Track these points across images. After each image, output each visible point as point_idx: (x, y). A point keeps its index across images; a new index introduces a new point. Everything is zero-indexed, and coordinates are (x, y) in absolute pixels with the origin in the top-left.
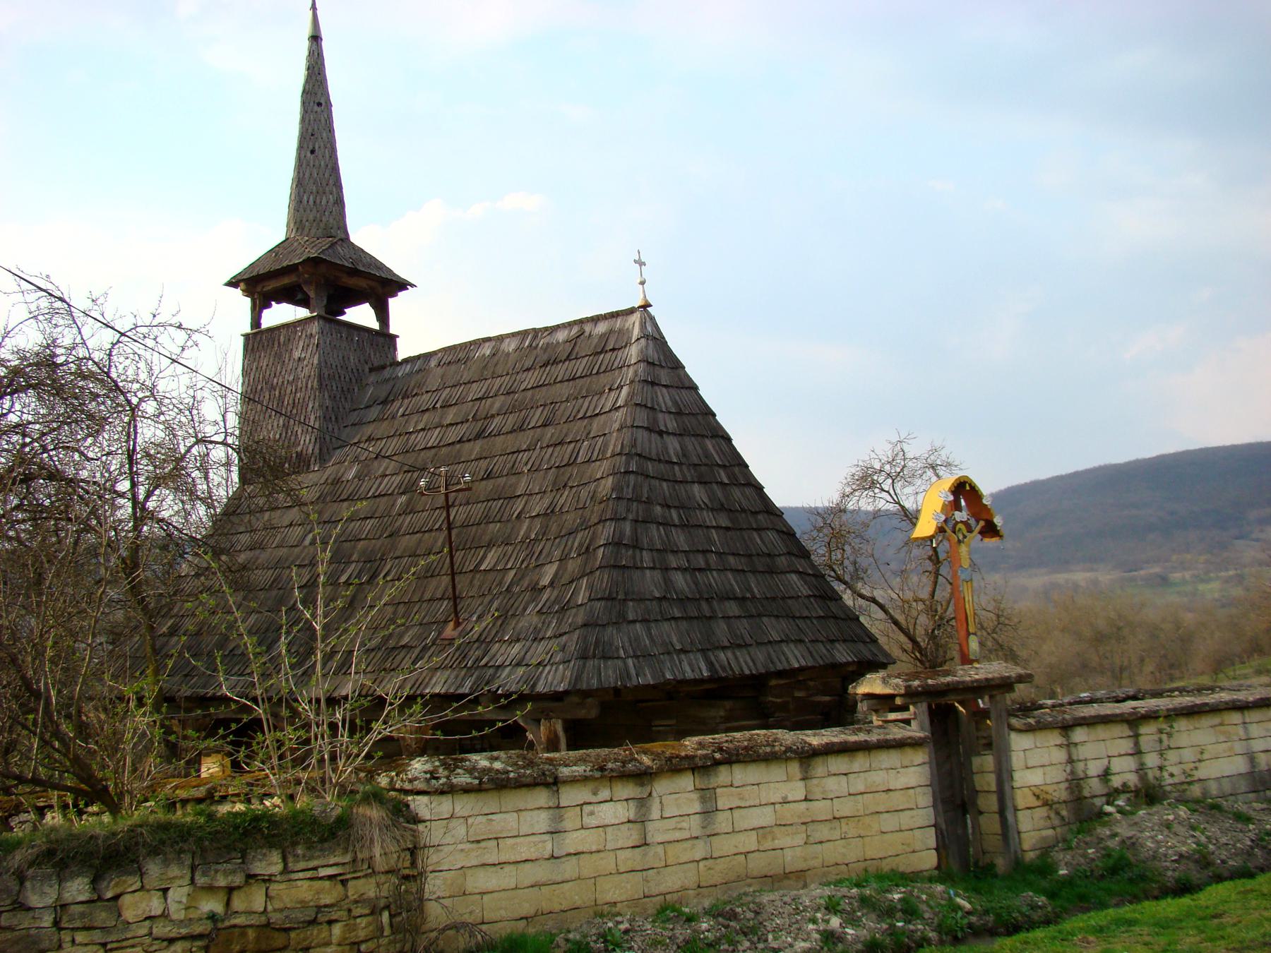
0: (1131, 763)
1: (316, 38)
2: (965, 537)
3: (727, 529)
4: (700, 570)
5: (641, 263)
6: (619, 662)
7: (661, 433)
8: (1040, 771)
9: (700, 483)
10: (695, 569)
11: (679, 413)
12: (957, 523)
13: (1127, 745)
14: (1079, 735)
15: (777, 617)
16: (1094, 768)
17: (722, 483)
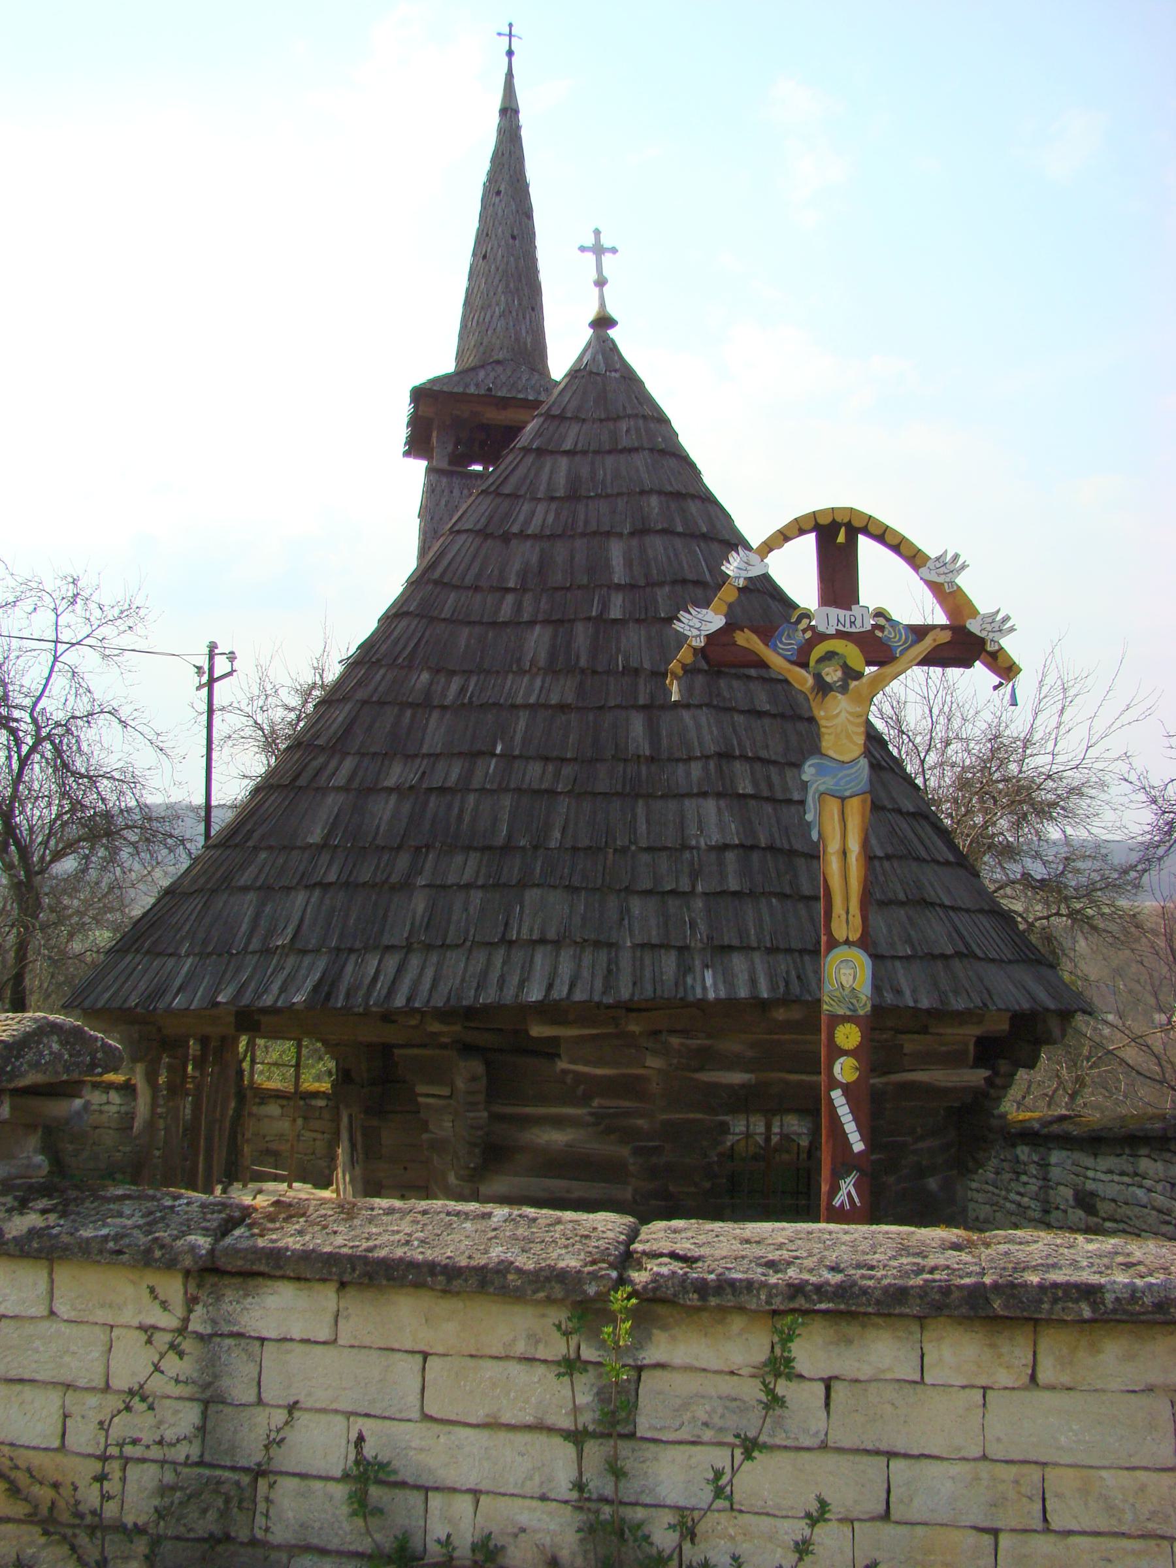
0: (559, 1464)
1: (509, 111)
2: (851, 674)
3: (563, 708)
4: (442, 790)
5: (599, 250)
6: (171, 962)
7: (506, 538)
8: (48, 1405)
9: (547, 622)
10: (430, 790)
11: (573, 496)
12: (820, 637)
13: (564, 1399)
14: (277, 1310)
15: (572, 889)
16: (321, 1445)
17: (602, 622)
